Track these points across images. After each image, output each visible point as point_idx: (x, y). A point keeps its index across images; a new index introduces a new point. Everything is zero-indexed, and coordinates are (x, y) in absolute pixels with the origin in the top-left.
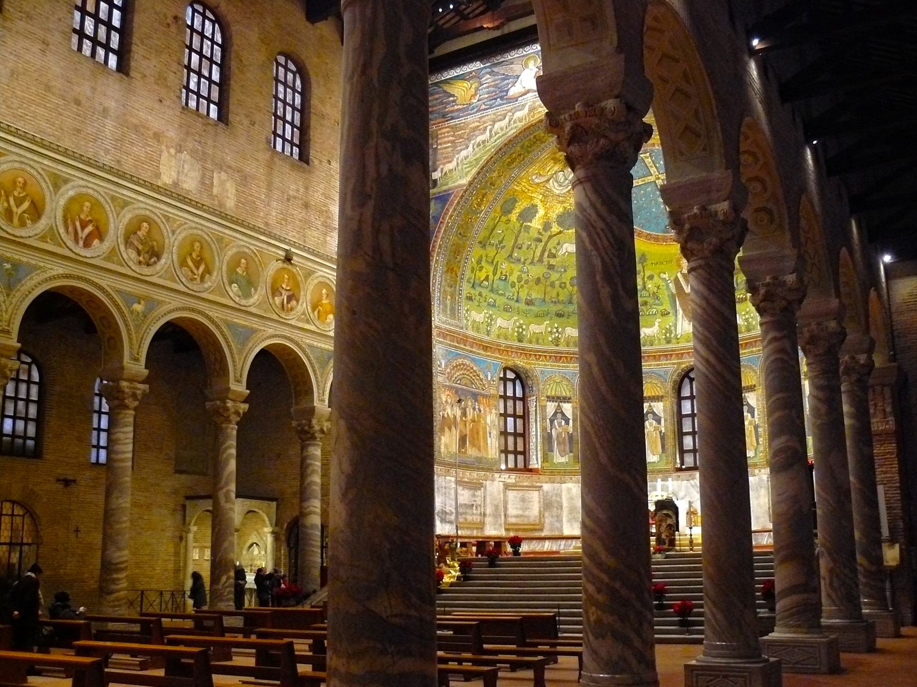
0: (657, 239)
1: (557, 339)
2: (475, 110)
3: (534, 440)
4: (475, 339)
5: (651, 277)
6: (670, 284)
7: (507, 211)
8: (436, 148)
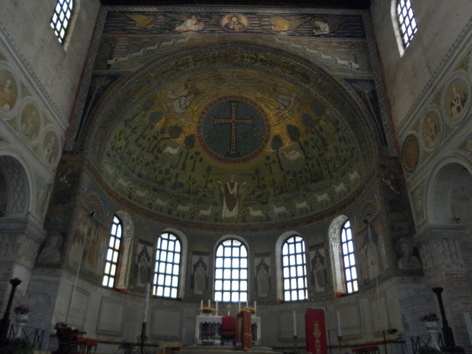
0: (220, 159)
1: (151, 204)
2: (149, 32)
3: (125, 268)
5: (211, 181)
6: (222, 188)
7: (146, 109)
8: (114, 47)
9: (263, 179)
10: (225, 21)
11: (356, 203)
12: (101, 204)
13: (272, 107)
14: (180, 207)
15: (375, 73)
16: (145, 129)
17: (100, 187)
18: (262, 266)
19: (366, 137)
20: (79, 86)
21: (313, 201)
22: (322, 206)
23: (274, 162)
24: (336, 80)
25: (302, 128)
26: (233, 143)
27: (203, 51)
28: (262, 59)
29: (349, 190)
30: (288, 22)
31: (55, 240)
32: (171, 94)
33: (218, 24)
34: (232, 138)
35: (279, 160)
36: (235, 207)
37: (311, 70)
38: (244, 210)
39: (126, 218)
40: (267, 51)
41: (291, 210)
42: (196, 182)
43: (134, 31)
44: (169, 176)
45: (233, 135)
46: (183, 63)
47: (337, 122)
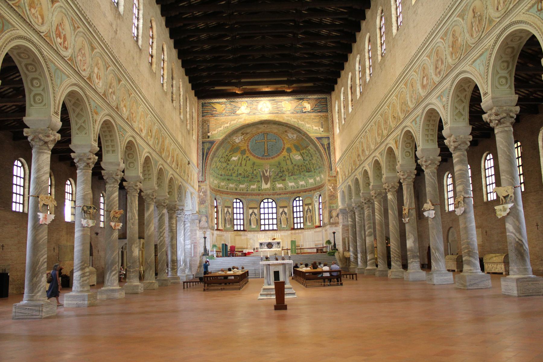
0: (259, 158)
1: (227, 187)
5: (255, 170)
9: (282, 168)
14: (241, 186)
18: (283, 213)
20: (198, 148)
23: (288, 159)
30: (290, 105)
31: (204, 219)
33: (256, 109)
35: (290, 159)
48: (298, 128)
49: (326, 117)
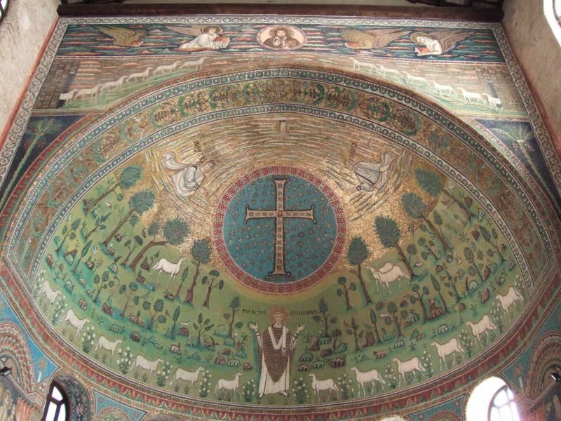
0: (255, 285)
4: (37, 316)
5: (239, 325)
6: (259, 338)
7: (125, 184)
9: (333, 321)
10: (265, 35)
11: (520, 349)
12: (27, 356)
13: (348, 185)
14: (182, 374)
15: (529, 113)
16: (121, 224)
17: (28, 322)
19: (530, 219)
21: (430, 356)
22: (450, 363)
23: (353, 287)
24: (464, 123)
25: (402, 222)
26: (279, 255)
27: (229, 79)
28: (330, 95)
29: (501, 328)
32: (170, 159)
33: (254, 40)
34: (277, 246)
35: (363, 284)
36: (284, 374)
37: (419, 110)
38: (301, 379)
39: (77, 390)
40: (339, 80)
41: (390, 376)
42: (213, 325)
43: (109, 52)
44: (163, 313)
45: (278, 239)
46: (192, 101)
47: (469, 201)
48: (407, 92)
49: (502, 73)
